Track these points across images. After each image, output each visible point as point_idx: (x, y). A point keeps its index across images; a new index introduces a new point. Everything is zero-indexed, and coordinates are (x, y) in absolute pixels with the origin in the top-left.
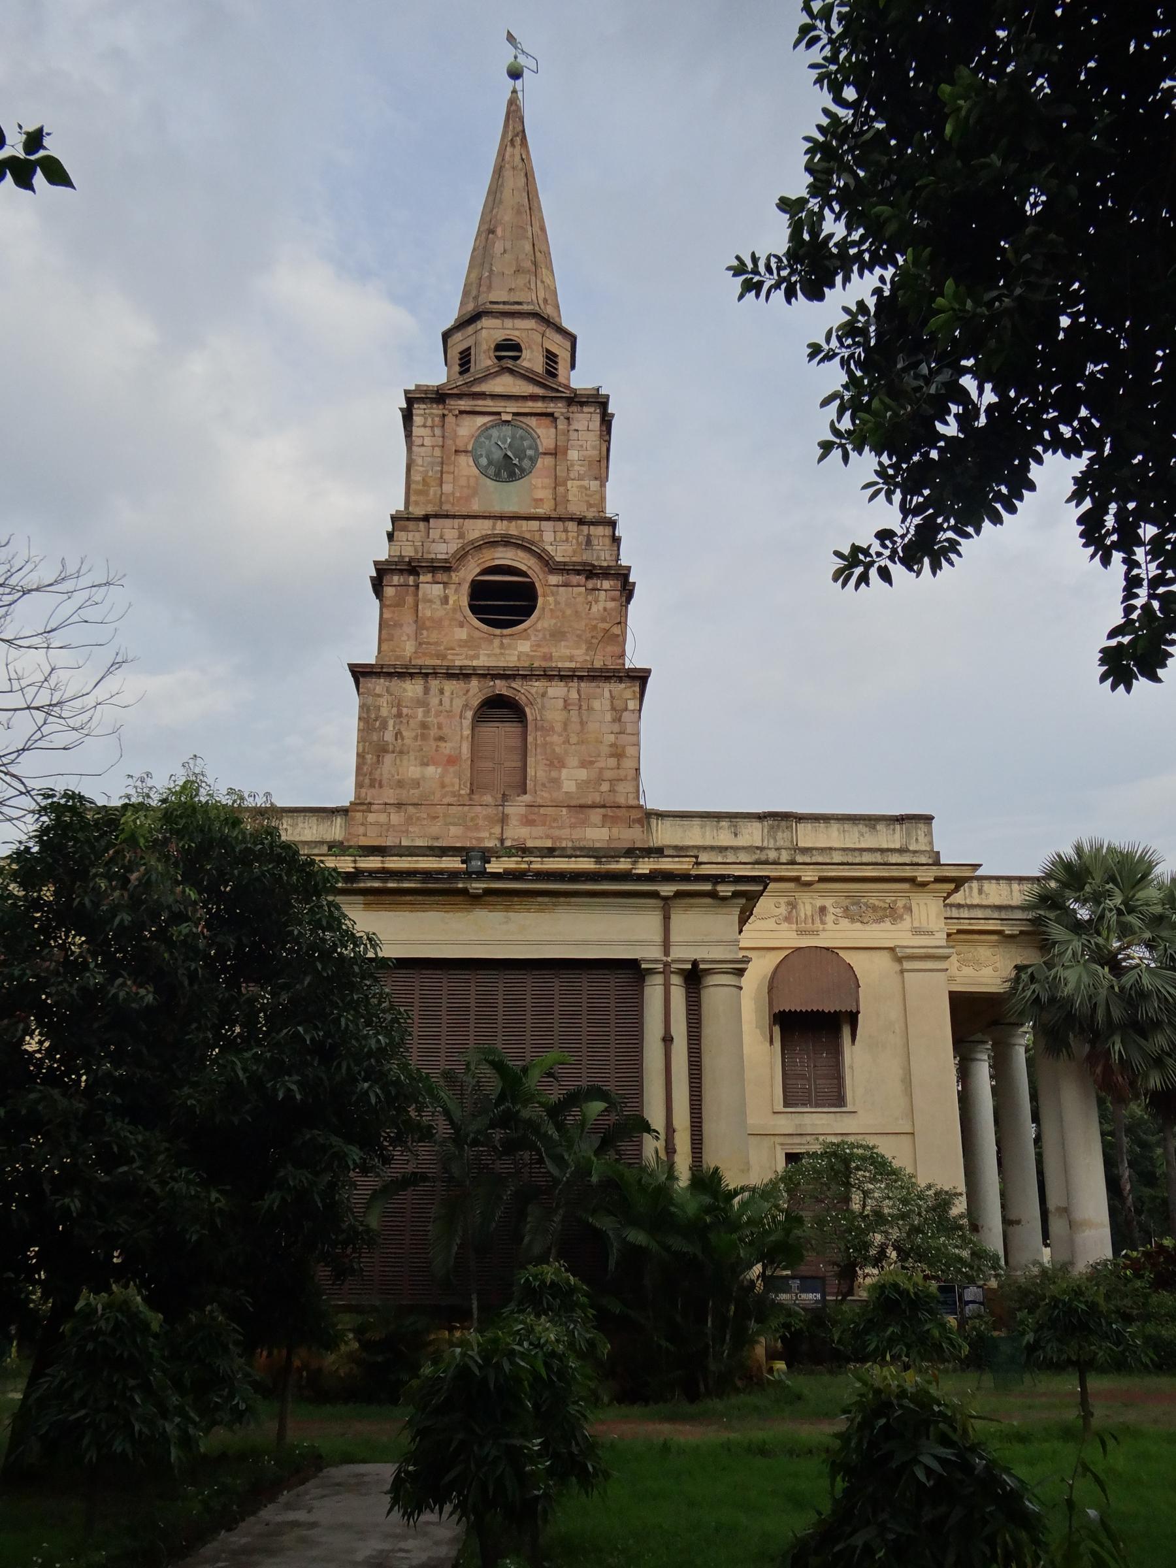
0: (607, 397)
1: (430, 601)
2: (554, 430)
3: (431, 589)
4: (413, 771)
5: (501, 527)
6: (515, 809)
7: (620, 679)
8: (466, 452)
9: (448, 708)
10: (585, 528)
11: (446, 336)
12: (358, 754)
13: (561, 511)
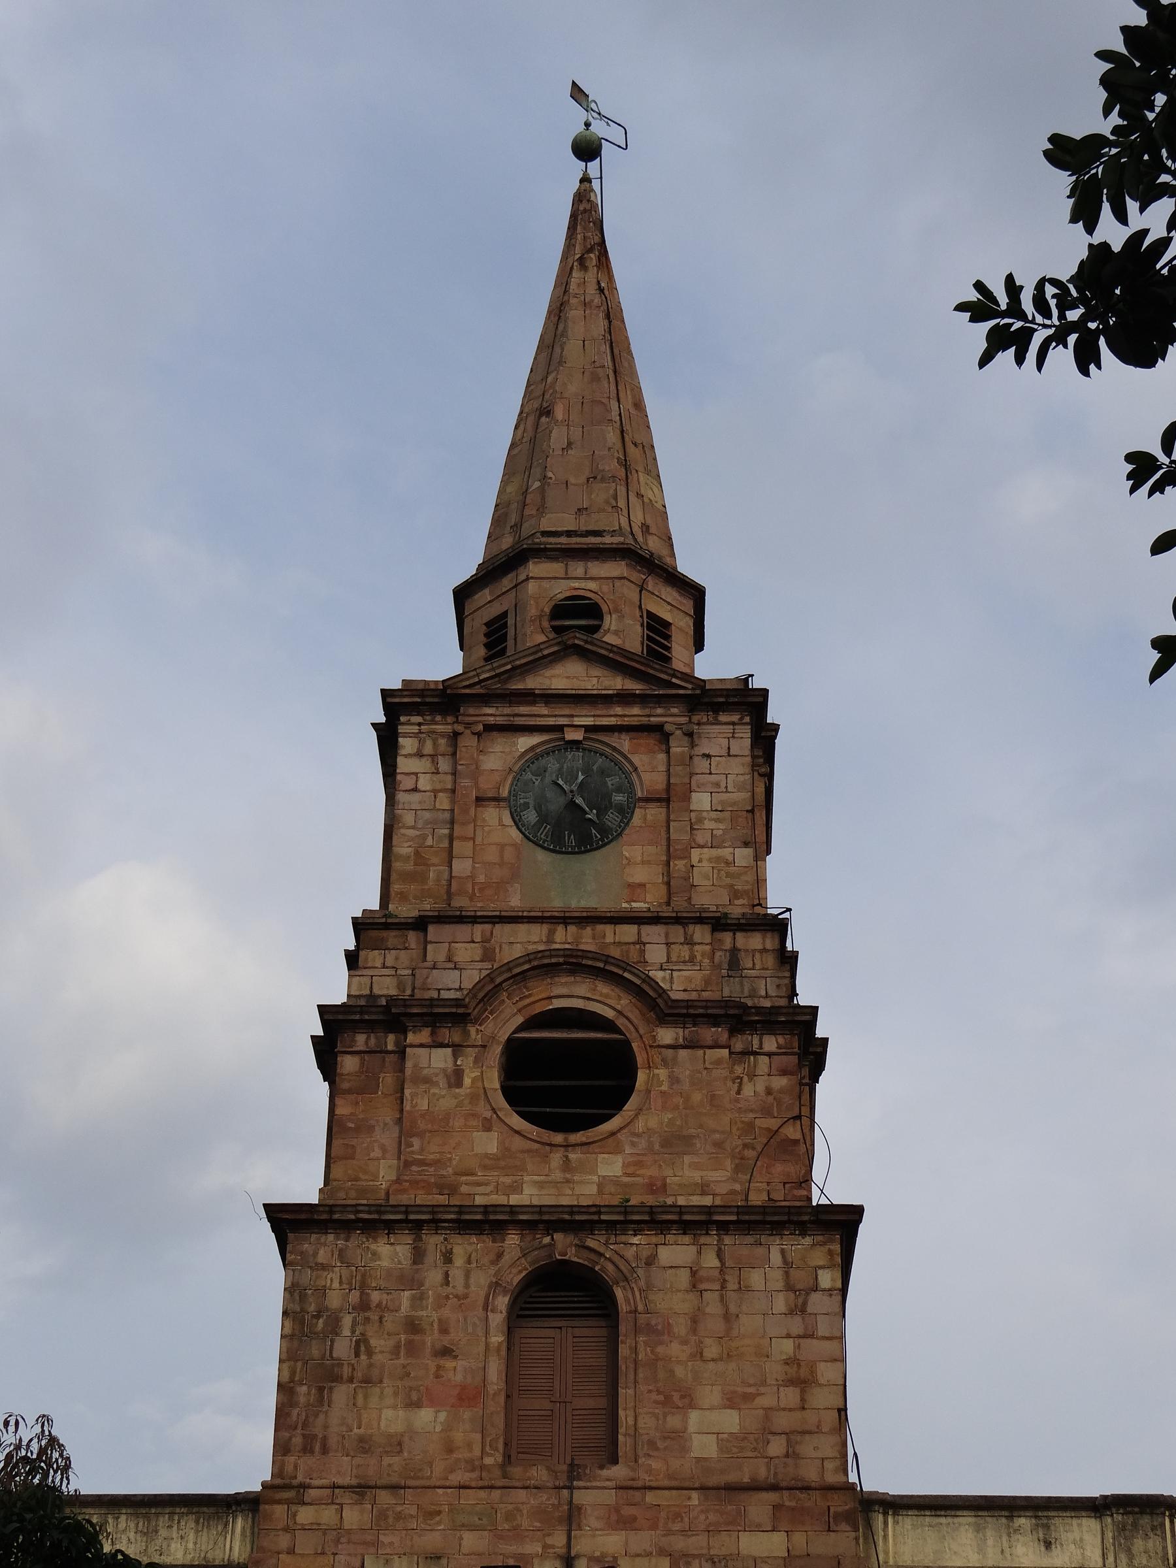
0: (764, 693)
1: (427, 1080)
2: (662, 757)
4: (388, 1417)
5: (563, 937)
6: (593, 1498)
7: (802, 1229)
8: (497, 799)
9: (460, 1290)
10: (727, 937)
11: (462, 595)
12: (280, 1385)
13: (679, 903)
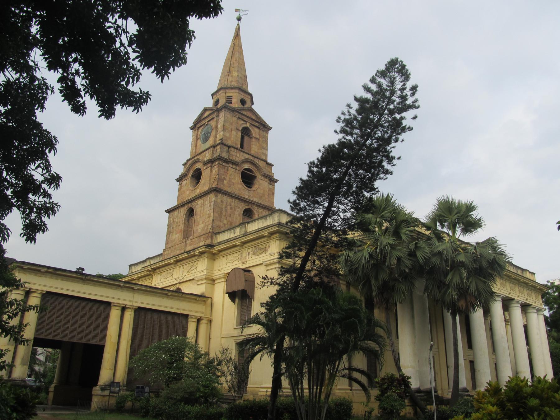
3: (184, 182)
